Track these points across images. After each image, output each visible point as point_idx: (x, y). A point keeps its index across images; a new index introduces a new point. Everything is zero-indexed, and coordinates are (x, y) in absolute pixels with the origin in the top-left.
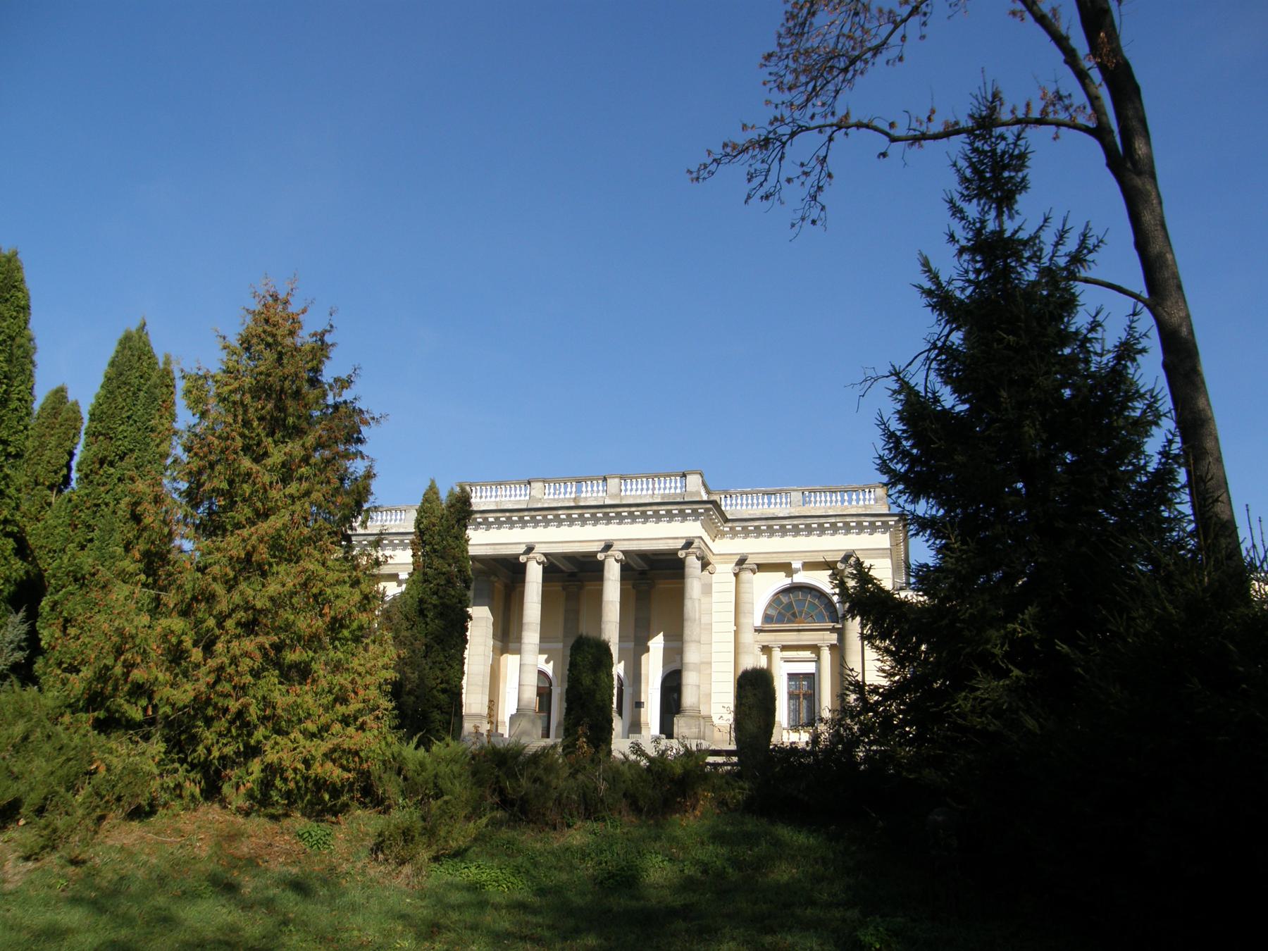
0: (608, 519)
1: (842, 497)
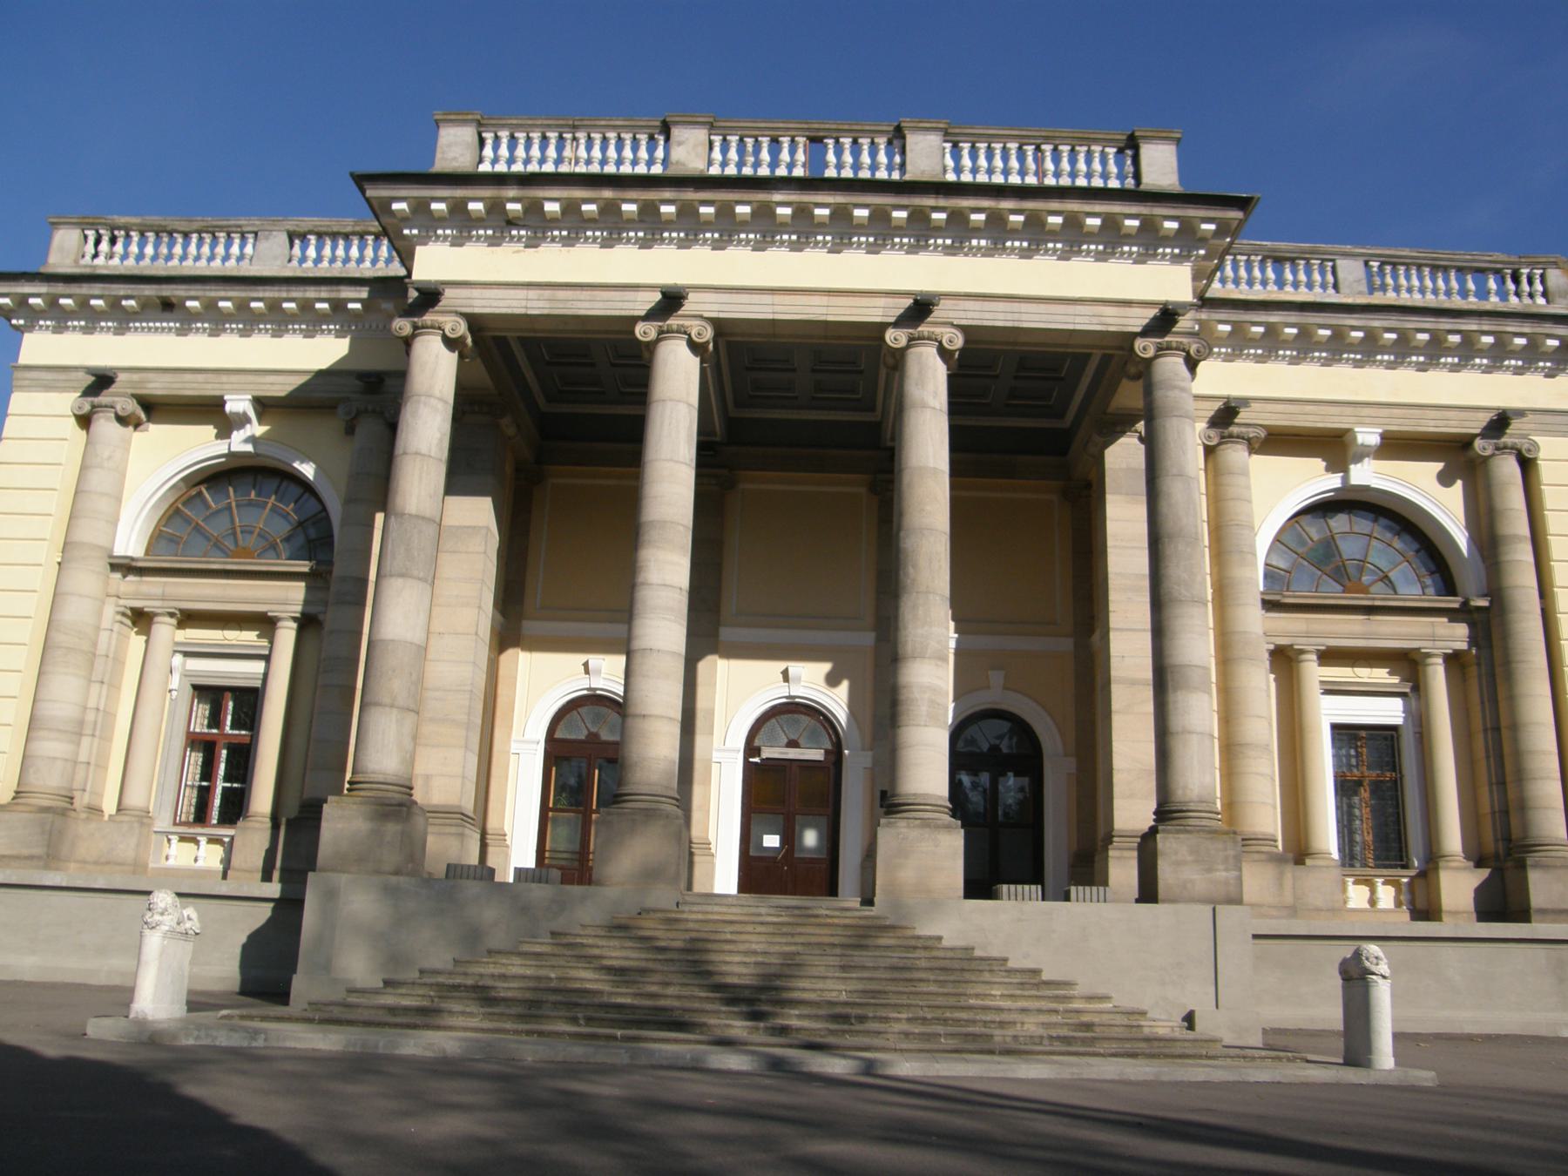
0: (920, 233)
1: (1462, 283)
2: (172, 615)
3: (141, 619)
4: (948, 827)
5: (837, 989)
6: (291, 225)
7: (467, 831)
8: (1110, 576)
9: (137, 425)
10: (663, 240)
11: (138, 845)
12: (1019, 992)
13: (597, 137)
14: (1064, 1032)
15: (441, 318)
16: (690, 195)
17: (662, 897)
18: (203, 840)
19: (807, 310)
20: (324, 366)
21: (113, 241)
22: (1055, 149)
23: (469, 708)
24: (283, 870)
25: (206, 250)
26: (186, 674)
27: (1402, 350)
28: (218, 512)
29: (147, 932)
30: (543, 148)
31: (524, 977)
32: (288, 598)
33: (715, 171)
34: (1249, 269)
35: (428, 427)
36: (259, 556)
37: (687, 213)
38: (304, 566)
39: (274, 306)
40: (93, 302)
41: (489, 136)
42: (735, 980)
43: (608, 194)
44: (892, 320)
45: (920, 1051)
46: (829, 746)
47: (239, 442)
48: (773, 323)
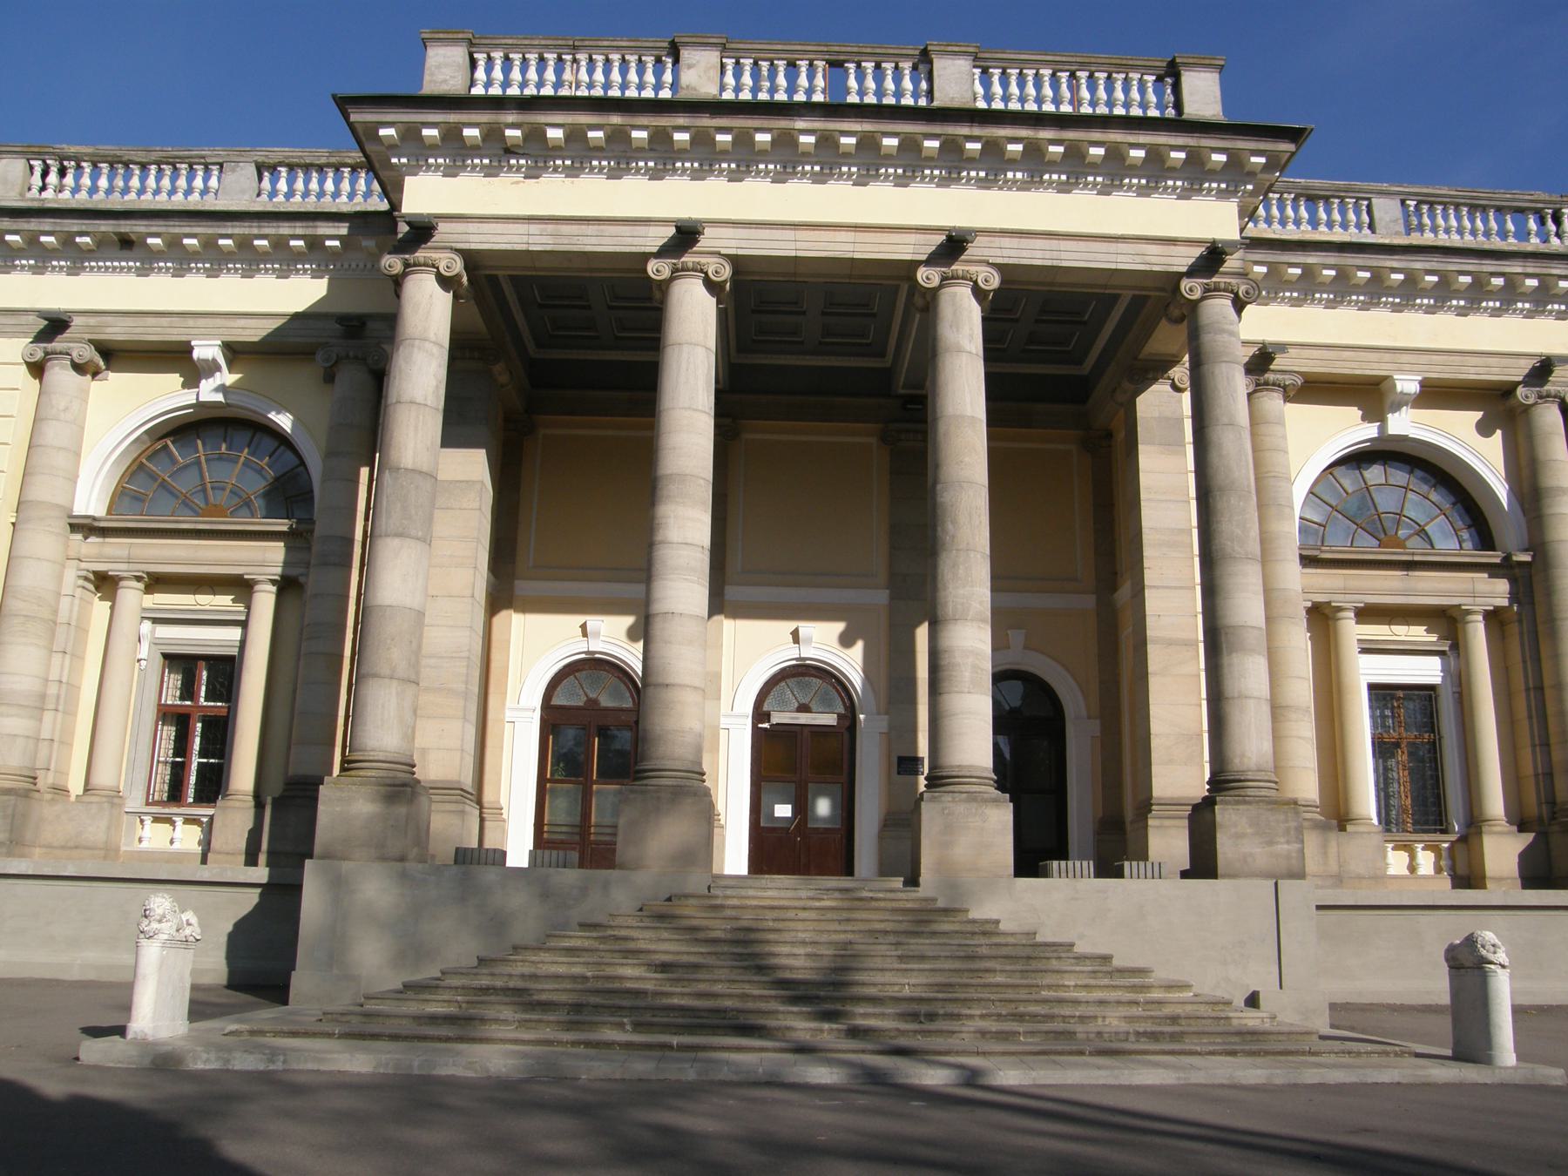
0: (952, 164)
2: (139, 579)
3: (105, 583)
4: (995, 800)
5: (910, 983)
6: (260, 156)
7: (468, 808)
8: (1144, 530)
9: (95, 374)
10: (675, 170)
11: (109, 828)
12: (1092, 982)
13: (599, 58)
14: (1149, 1027)
15: (434, 255)
16: (706, 121)
17: (695, 882)
18: (179, 821)
19: (831, 246)
20: (300, 310)
21: (62, 173)
22: (1091, 76)
23: (466, 677)
24: (270, 853)
25: (166, 182)
26: (156, 643)
27: (1443, 295)
28: (186, 467)
29: (144, 942)
30: (541, 70)
31: (557, 977)
32: (266, 559)
33: (728, 95)
34: (1282, 209)
35: (422, 373)
36: (232, 514)
37: (702, 140)
38: (282, 525)
39: (244, 244)
40: (43, 239)
41: (481, 57)
42: (788, 975)
43: (616, 119)
44: (924, 257)
45: (1004, 1054)
46: (842, 710)
47: (208, 391)
48: (796, 260)
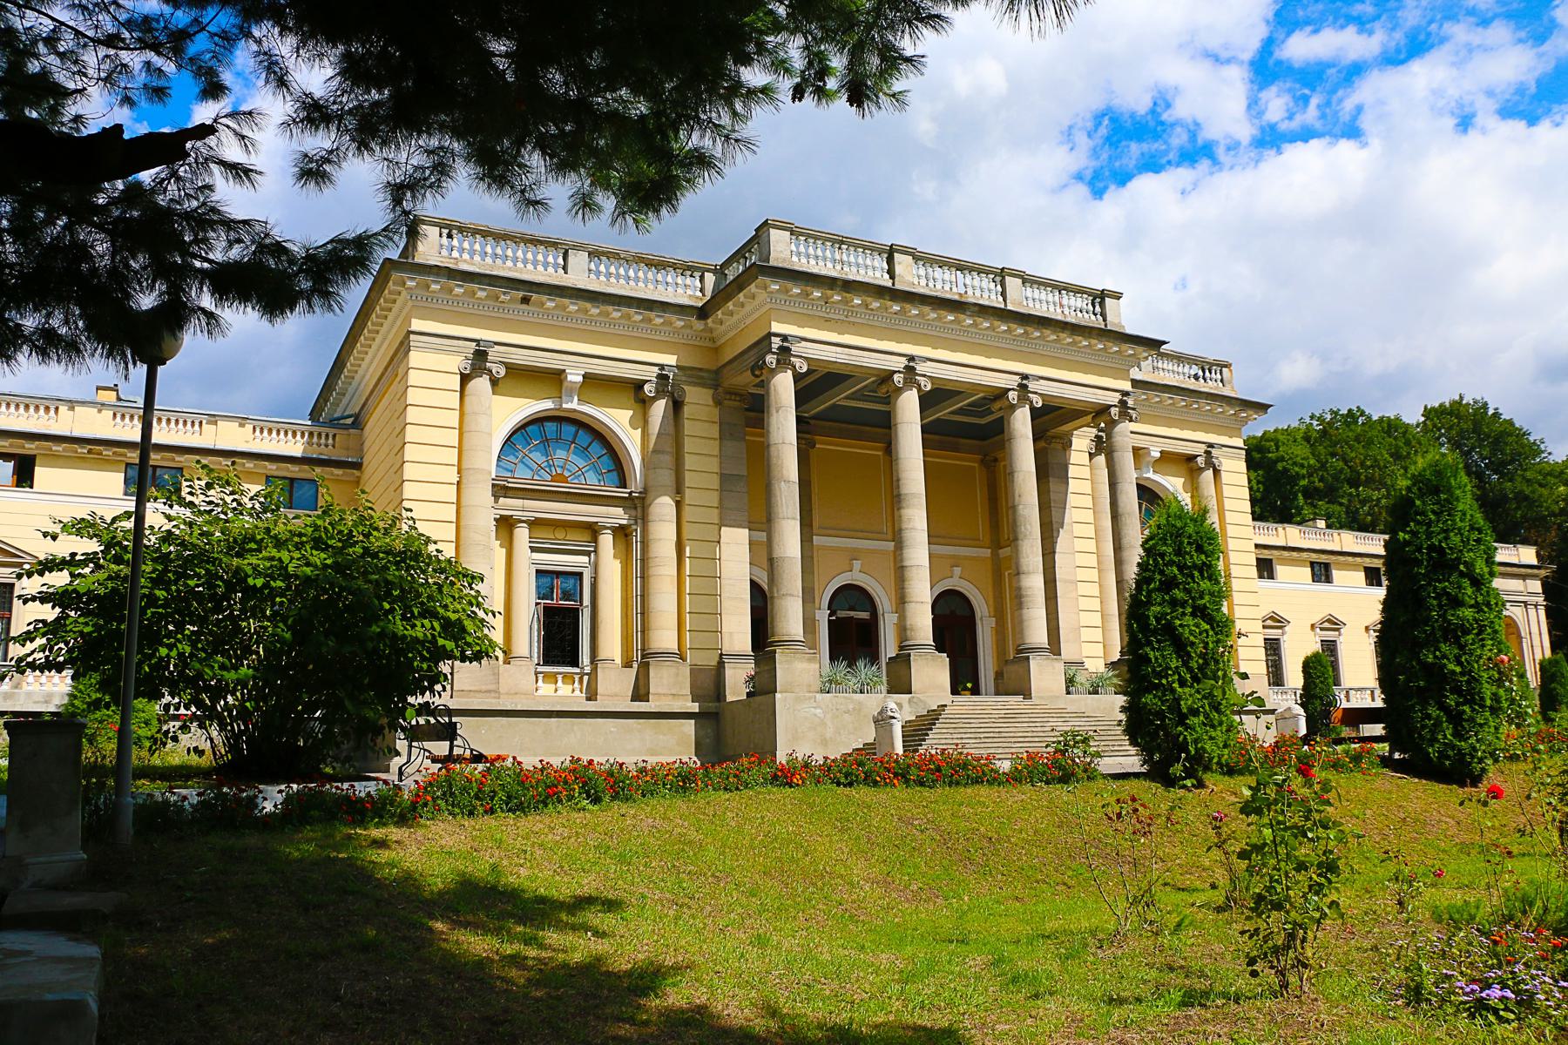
18: (560, 677)
